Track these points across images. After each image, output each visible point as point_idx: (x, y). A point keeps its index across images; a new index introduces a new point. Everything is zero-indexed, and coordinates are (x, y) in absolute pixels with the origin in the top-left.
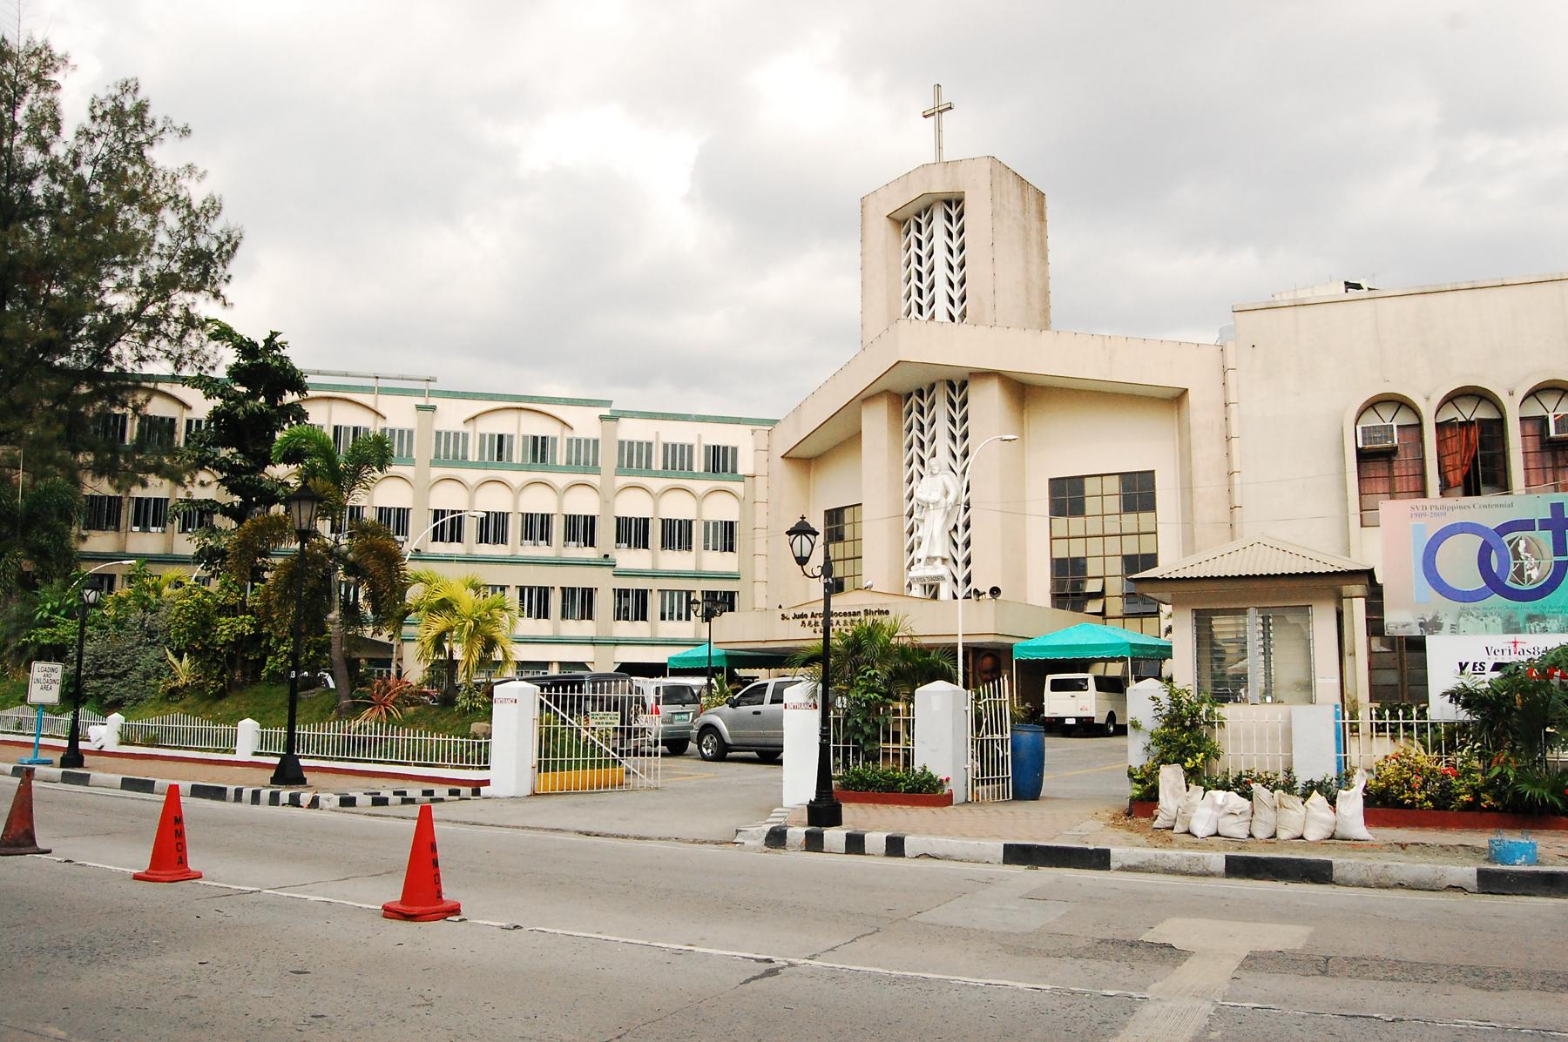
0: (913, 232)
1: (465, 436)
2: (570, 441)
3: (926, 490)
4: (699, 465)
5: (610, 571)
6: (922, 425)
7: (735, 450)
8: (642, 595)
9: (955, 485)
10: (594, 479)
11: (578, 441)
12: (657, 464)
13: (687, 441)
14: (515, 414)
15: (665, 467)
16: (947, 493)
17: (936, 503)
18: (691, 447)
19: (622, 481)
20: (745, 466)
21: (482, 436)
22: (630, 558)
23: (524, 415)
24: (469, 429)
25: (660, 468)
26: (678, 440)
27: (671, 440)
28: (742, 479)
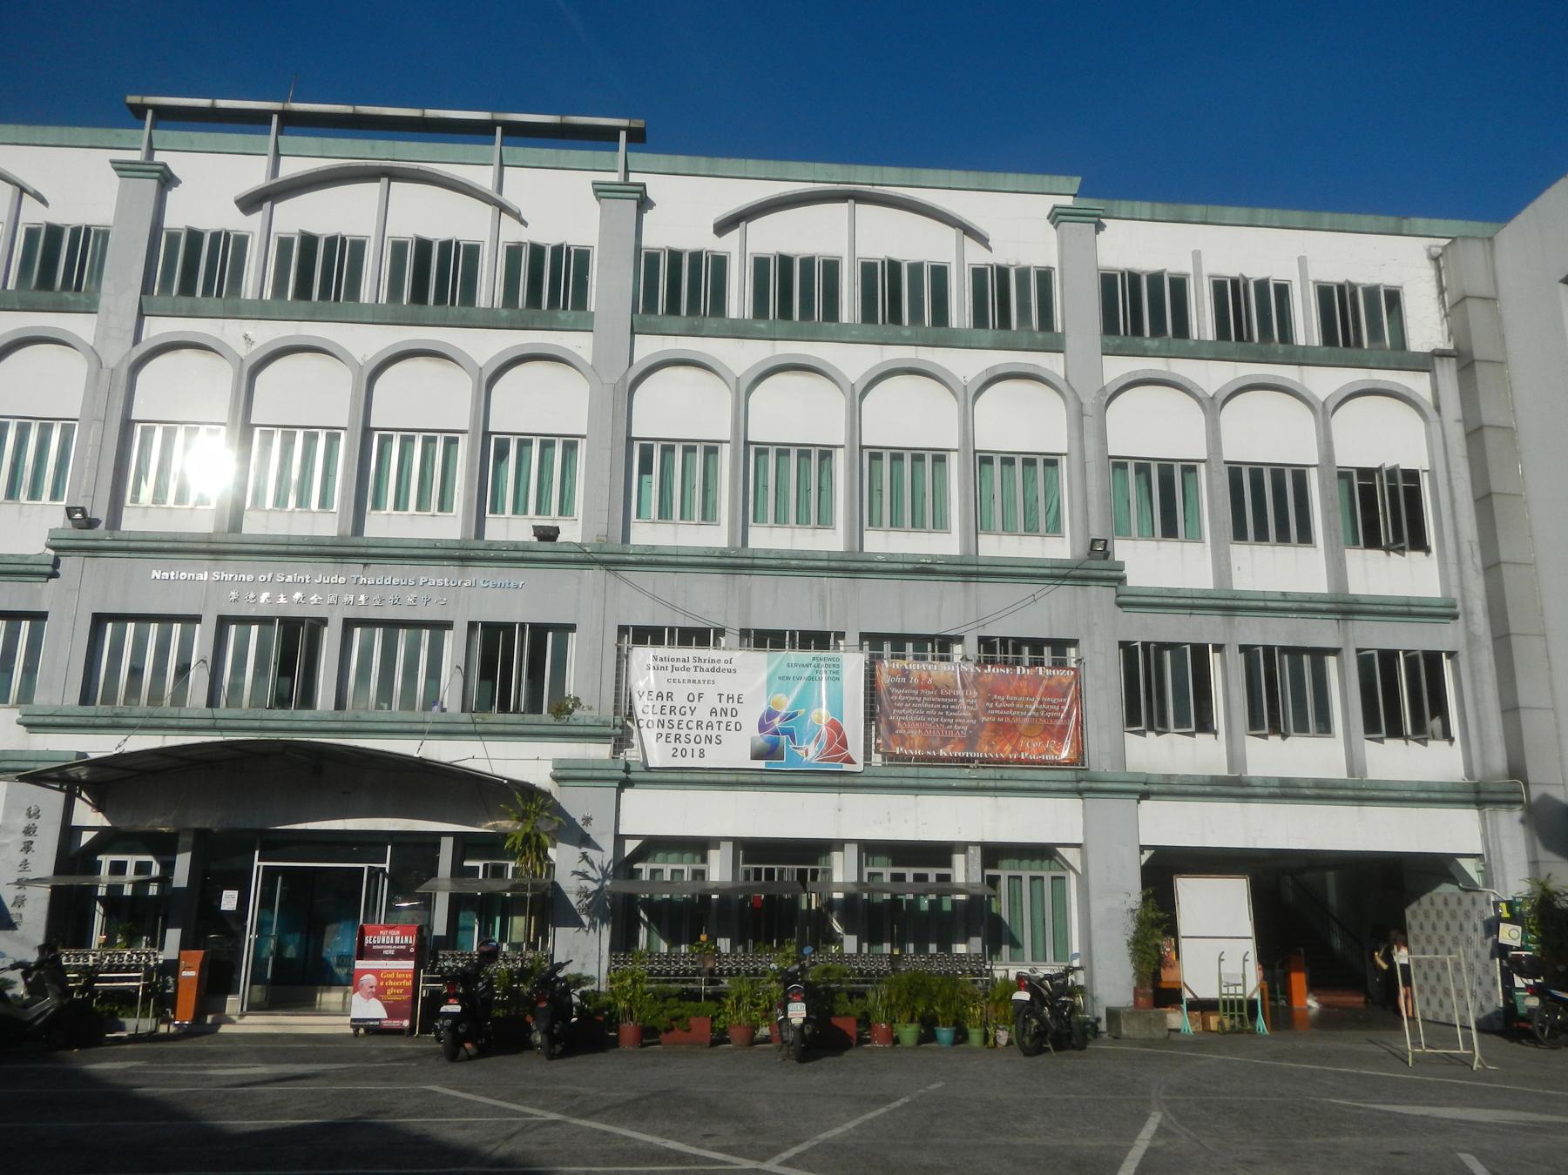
1: (720, 263)
2: (979, 274)
4: (1306, 327)
5: (1100, 596)
7: (1394, 297)
11: (1003, 272)
12: (1202, 322)
13: (1276, 271)
14: (843, 208)
15: (1222, 332)
18: (1283, 290)
19: (1118, 368)
20: (1425, 327)
21: (761, 264)
22: (1150, 563)
23: (863, 210)
24: (729, 244)
25: (1210, 334)
27: (1229, 269)
28: (1424, 363)
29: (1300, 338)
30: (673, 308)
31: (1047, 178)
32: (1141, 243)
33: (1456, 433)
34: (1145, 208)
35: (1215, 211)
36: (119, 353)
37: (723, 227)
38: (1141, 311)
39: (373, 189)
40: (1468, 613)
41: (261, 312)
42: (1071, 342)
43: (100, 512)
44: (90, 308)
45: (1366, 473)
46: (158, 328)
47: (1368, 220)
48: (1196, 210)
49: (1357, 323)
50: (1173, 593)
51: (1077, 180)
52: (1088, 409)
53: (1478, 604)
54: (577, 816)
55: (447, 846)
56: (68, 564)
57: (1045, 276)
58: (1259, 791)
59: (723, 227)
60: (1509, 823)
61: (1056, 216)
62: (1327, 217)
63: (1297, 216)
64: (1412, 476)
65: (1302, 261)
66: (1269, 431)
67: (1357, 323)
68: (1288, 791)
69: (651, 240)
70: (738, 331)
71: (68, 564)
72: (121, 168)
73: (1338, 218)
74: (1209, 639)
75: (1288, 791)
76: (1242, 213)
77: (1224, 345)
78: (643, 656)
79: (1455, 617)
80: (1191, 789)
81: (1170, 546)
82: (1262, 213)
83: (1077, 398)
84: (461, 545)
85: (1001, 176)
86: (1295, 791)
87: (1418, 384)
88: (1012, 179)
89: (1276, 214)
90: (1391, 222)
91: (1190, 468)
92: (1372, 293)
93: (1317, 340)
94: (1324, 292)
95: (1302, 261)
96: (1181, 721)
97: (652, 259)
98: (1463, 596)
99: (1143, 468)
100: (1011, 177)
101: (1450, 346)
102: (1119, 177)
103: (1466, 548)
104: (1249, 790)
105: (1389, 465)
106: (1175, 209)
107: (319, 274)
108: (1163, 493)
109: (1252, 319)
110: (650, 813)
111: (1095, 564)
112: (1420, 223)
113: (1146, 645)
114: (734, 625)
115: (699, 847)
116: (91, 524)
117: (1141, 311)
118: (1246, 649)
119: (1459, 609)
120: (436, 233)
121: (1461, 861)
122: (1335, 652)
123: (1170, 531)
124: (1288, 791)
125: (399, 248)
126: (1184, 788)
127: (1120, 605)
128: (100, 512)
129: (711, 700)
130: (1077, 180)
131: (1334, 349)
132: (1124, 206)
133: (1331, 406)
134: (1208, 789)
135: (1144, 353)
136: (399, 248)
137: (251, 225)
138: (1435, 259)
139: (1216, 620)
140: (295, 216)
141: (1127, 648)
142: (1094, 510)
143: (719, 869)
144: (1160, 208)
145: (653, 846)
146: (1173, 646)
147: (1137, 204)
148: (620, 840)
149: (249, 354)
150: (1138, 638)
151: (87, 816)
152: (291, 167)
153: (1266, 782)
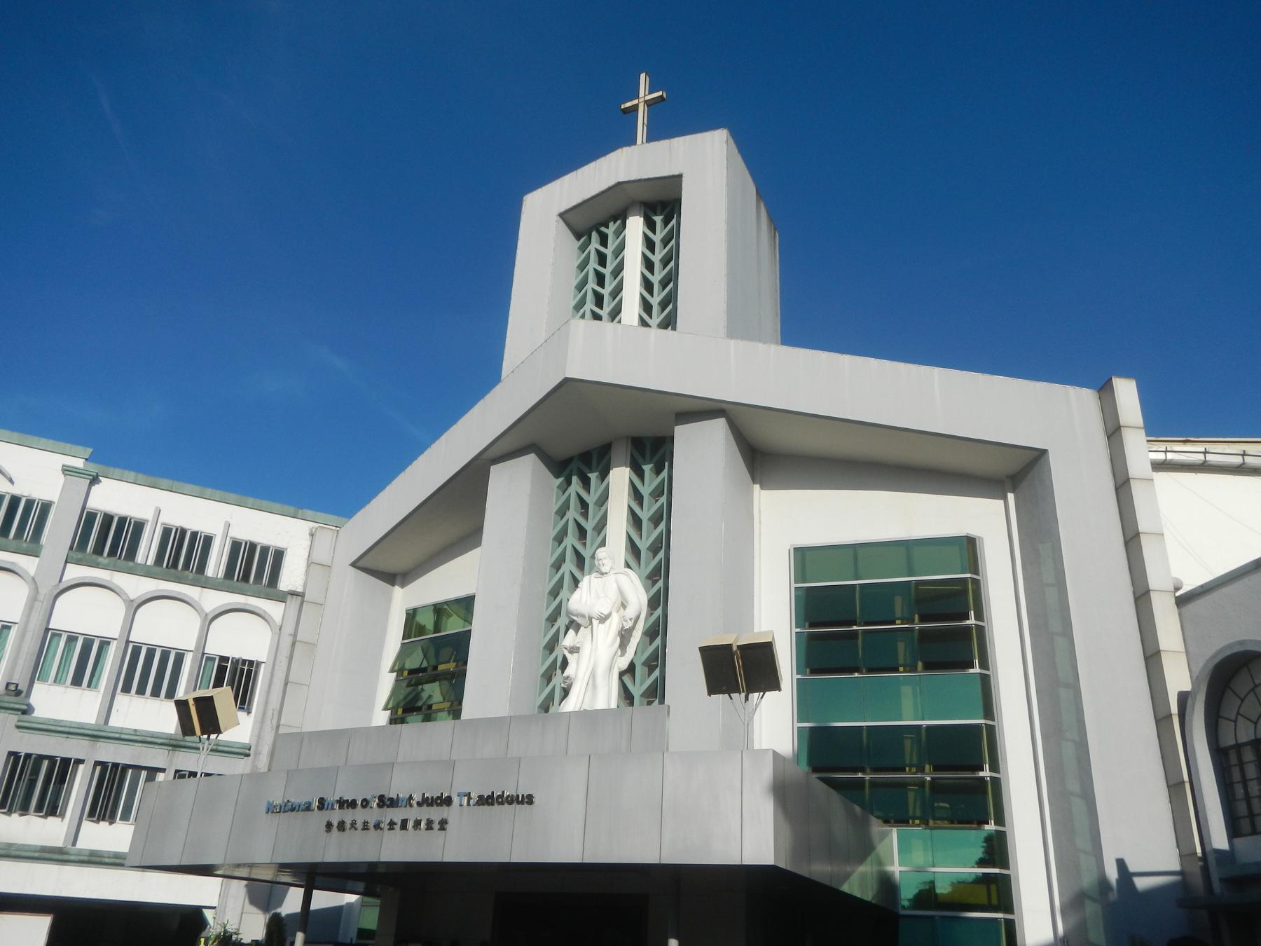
0: (595, 244)
3: (589, 596)
4: (216, 565)
6: (584, 505)
7: (279, 555)
8: (63, 769)
9: (638, 597)
10: (27, 564)
16: (624, 606)
17: (603, 619)
18: (208, 540)
19: (75, 572)
20: (291, 577)
22: (56, 702)
26: (192, 525)
28: (282, 597)
29: (210, 571)
31: (69, 445)
32: (118, 497)
33: (286, 641)
34: (132, 475)
35: (177, 484)
38: (108, 540)
40: (257, 753)
42: (44, 552)
45: (224, 659)
47: (277, 506)
48: (165, 482)
49: (253, 568)
50: (57, 722)
51: (90, 450)
52: (41, 597)
53: (265, 749)
57: (46, 507)
58: (73, 858)
60: (238, 889)
61: (67, 470)
62: (251, 500)
63: (232, 496)
64: (251, 663)
65: (228, 526)
66: (171, 623)
67: (253, 568)
68: (95, 859)
73: (258, 501)
74: (73, 754)
75: (93, 859)
76: (197, 489)
77: (158, 569)
79: (248, 755)
80: (23, 854)
81: (76, 691)
82: (209, 491)
83: (37, 588)
85: (36, 438)
86: (98, 859)
87: (274, 609)
88: (43, 441)
89: (219, 493)
90: (292, 509)
91: (105, 643)
92: (265, 550)
93: (221, 574)
94: (236, 545)
95: (228, 526)
96: (39, 808)
98: (257, 746)
99: (72, 639)
100: (43, 440)
101: (300, 590)
102: (113, 454)
103: (269, 713)
104: (65, 857)
105: (237, 656)
106: (151, 479)
108: (84, 659)
109: (182, 555)
111: (7, 698)
112: (309, 513)
113: (28, 756)
117: (108, 540)
118: (103, 764)
119: (252, 752)
121: (205, 911)
122: (163, 770)
123: (77, 681)
124: (95, 859)
126: (18, 853)
127: (18, 727)
130: (90, 450)
131: (228, 582)
132: (117, 472)
133: (210, 617)
134: (36, 855)
135: (97, 566)
138: (312, 535)
139: (85, 742)
141: (14, 755)
142: (21, 662)
144: (141, 477)
146: (52, 759)
147: (126, 472)
150: (23, 750)
153: (80, 852)
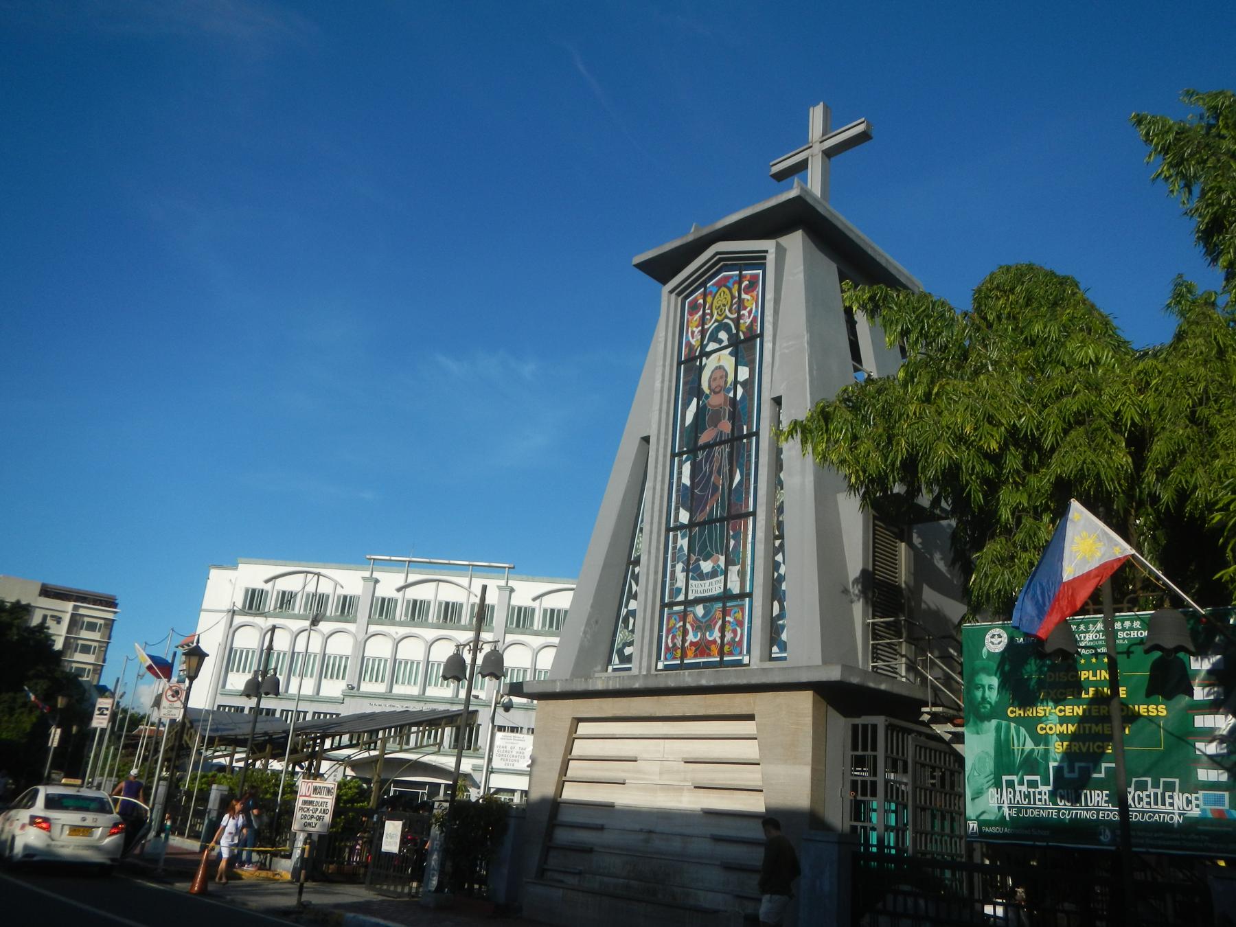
1: (533, 610)
24: (536, 604)
30: (518, 625)
36: (361, 637)
37: (534, 599)
39: (434, 584)
41: (401, 624)
43: (355, 685)
44: (354, 621)
46: (373, 628)
54: (478, 781)
55: (442, 787)
56: (347, 699)
59: (534, 599)
69: (513, 602)
70: (537, 633)
71: (347, 699)
72: (364, 579)
78: (499, 735)
84: (452, 699)
97: (513, 608)
107: (417, 610)
110: (497, 781)
114: (526, 727)
115: (513, 791)
116: (353, 688)
120: (451, 599)
125: (440, 604)
128: (355, 685)
129: (517, 749)
136: (440, 604)
137: (399, 595)
140: (412, 593)
143: (517, 799)
145: (499, 791)
148: (487, 788)
149: (398, 637)
151: (350, 772)
152: (413, 578)
